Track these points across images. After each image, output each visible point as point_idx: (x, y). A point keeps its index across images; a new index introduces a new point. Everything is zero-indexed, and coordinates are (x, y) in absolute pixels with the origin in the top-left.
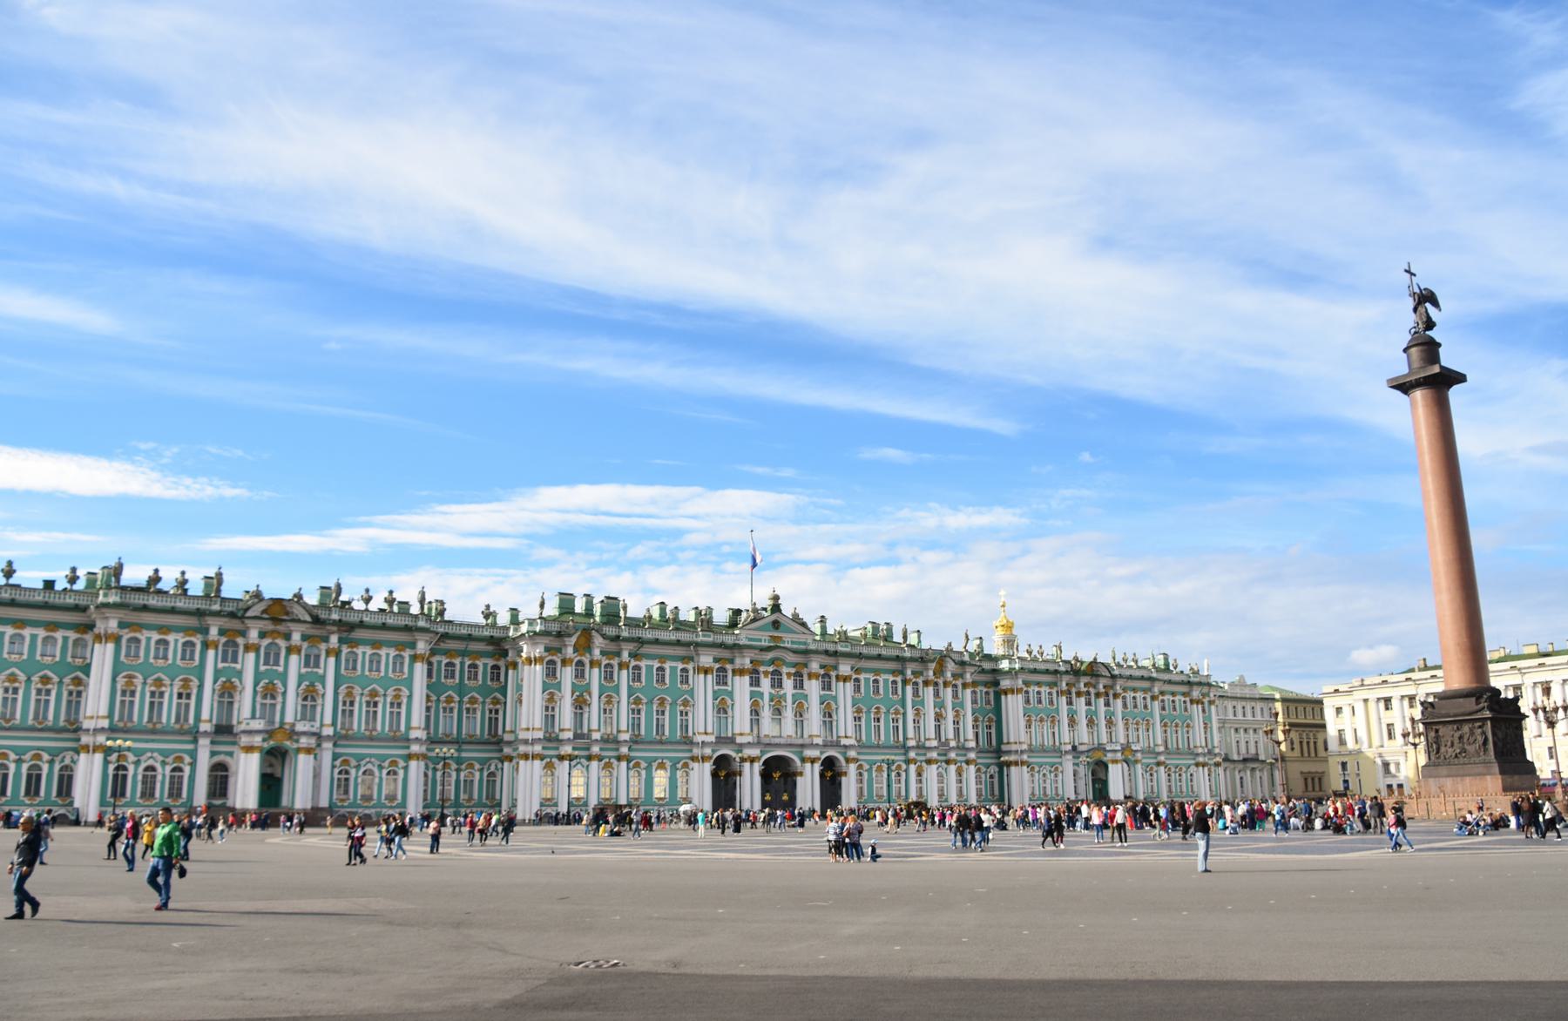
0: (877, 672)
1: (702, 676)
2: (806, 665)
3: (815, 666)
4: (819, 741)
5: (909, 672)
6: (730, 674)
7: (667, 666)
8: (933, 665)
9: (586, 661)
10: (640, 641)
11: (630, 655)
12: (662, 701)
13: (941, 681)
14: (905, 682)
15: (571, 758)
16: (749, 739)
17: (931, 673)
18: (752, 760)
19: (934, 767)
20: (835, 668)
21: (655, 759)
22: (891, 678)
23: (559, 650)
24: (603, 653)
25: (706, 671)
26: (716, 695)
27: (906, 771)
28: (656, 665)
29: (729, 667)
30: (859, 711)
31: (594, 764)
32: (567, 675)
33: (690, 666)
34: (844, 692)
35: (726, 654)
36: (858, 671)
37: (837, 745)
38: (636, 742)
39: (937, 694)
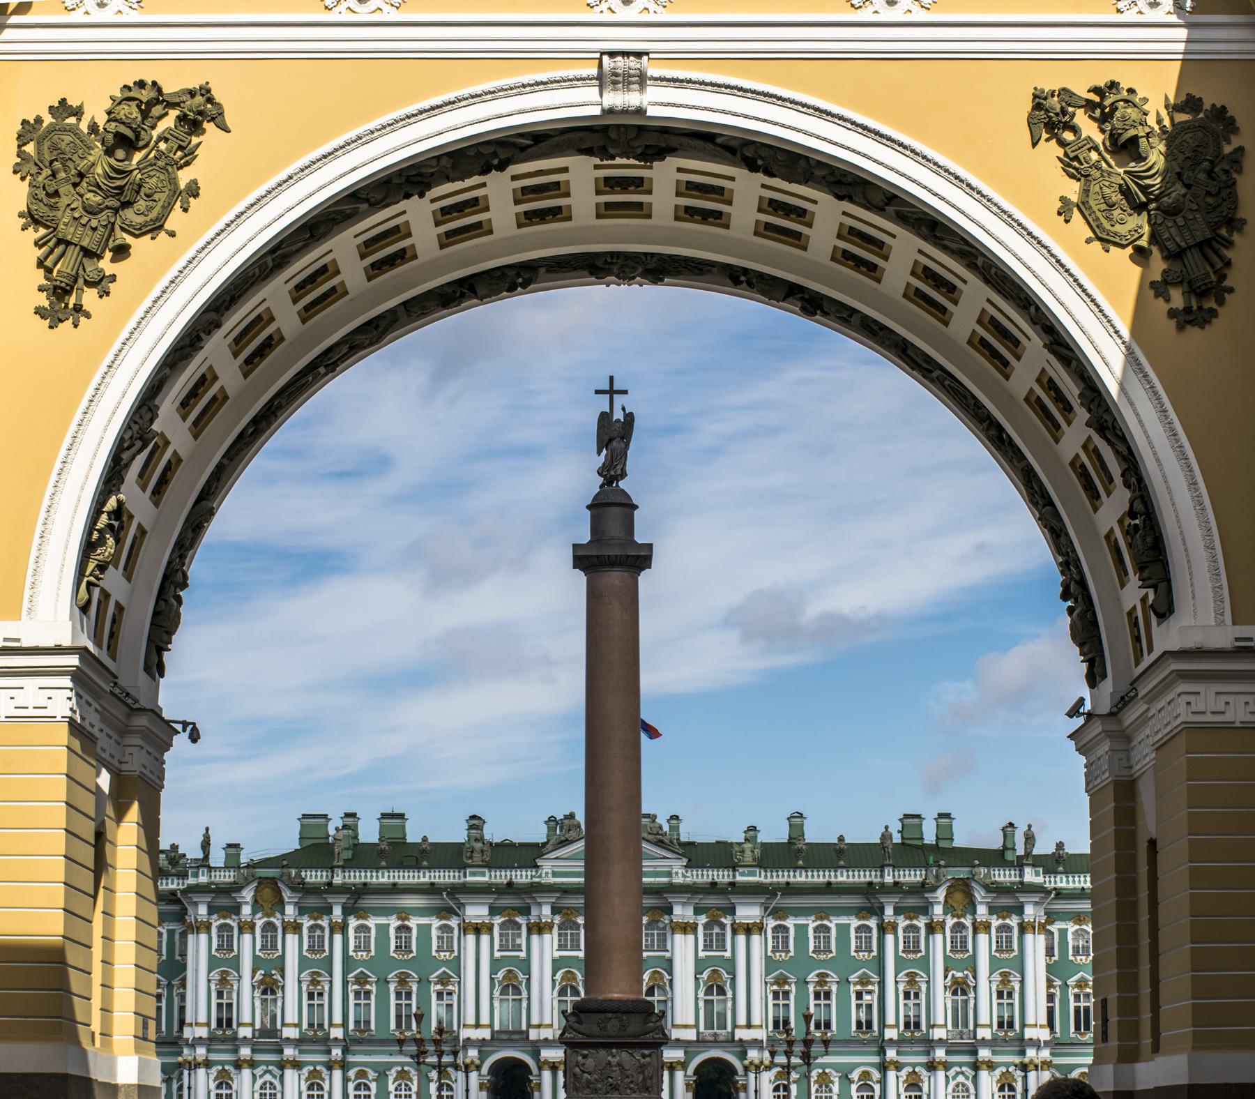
0: (822, 913)
1: (471, 939)
2: (669, 911)
3: (682, 912)
4: (690, 1035)
5: (889, 911)
6: (524, 929)
7: (413, 923)
8: (941, 894)
9: (278, 924)
10: (365, 890)
11: (347, 912)
12: (403, 980)
13: (968, 921)
14: (882, 929)
15: (252, 1064)
16: (547, 1034)
17: (938, 910)
18: (554, 1067)
19: (941, 1074)
20: (732, 911)
21: (390, 1066)
22: (855, 923)
23: (236, 909)
24: (302, 911)
25: (478, 930)
26: (495, 964)
27: (883, 1082)
28: (394, 923)
29: (519, 919)
30: (781, 981)
31: (290, 1074)
32: (247, 947)
33: (454, 922)
34: (750, 956)
35: (506, 901)
36: (777, 913)
37: (731, 1040)
38: (360, 1042)
39: (959, 945)
